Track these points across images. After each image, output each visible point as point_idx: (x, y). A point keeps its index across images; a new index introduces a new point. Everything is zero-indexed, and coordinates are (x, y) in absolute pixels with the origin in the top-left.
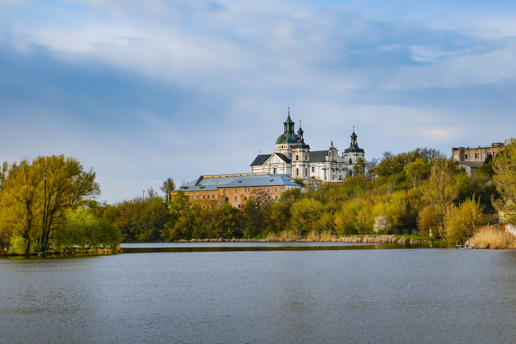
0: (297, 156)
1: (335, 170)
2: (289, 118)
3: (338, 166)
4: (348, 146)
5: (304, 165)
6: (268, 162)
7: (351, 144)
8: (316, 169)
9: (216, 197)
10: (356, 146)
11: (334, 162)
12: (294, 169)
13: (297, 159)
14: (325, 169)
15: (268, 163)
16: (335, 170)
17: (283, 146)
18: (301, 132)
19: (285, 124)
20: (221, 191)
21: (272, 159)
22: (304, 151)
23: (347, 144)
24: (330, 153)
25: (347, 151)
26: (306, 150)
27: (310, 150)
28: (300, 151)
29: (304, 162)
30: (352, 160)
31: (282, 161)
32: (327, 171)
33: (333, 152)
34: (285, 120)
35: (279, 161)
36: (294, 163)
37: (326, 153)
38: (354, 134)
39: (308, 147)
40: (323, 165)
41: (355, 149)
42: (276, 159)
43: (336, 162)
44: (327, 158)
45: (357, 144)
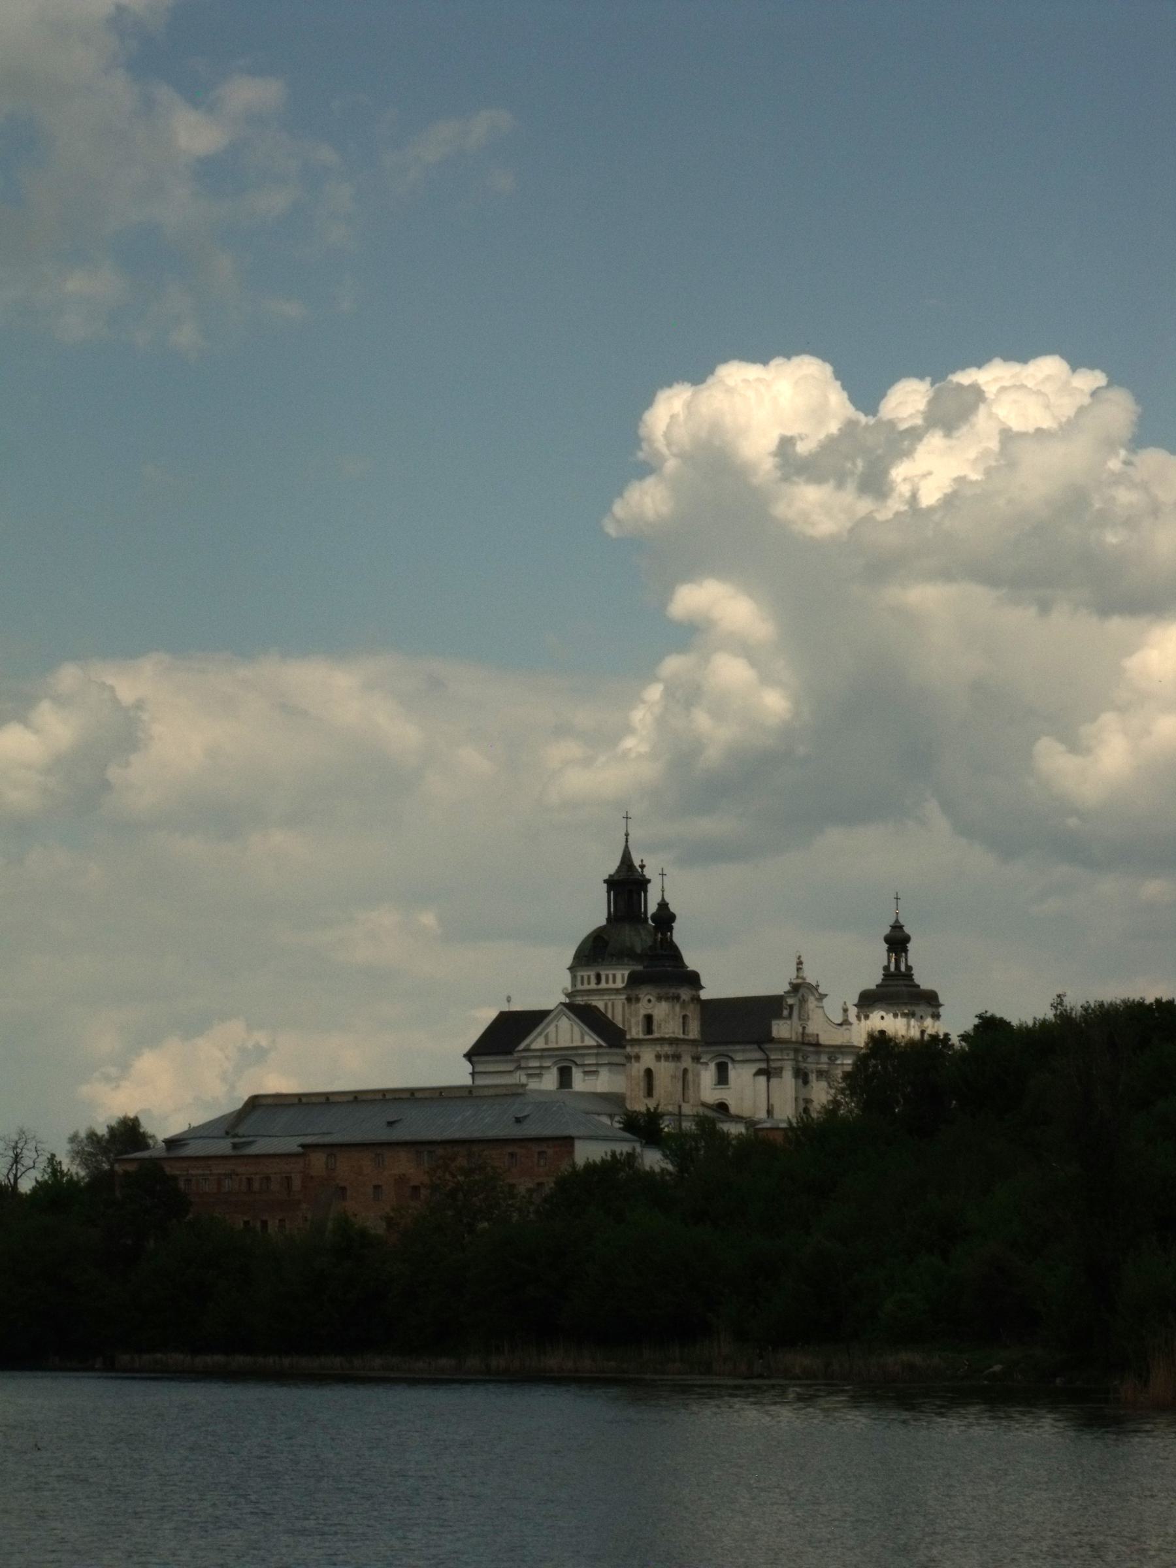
0: (649, 1019)
1: (813, 1077)
2: (626, 859)
3: (824, 1059)
4: (872, 979)
5: (677, 1057)
7: (886, 968)
8: (732, 1073)
10: (908, 975)
11: (808, 1045)
12: (637, 1069)
13: (649, 1029)
14: (766, 1073)
15: (539, 1044)
17: (598, 978)
19: (612, 883)
20: (318, 1161)
21: (552, 1028)
22: (677, 998)
23: (871, 967)
24: (791, 1007)
25: (868, 1001)
26: (685, 994)
27: (704, 995)
28: (659, 999)
29: (673, 1041)
31: (591, 1040)
32: (774, 1081)
33: (803, 1001)
34: (611, 866)
35: (583, 1040)
36: (636, 1049)
37: (770, 1007)
38: (897, 927)
39: (693, 980)
40: (758, 1055)
41: (898, 989)
42: (567, 1033)
43: (818, 1045)
44: (781, 1029)
45: (909, 968)
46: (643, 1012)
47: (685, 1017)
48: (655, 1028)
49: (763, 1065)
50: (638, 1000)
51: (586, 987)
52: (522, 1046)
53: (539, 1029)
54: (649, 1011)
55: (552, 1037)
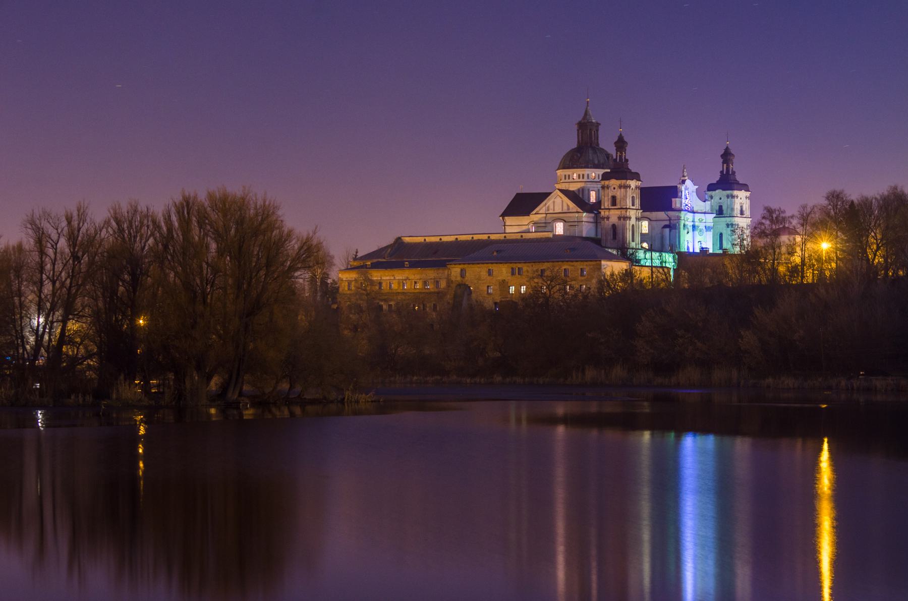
0: (614, 198)
2: (586, 113)
4: (715, 178)
6: (542, 208)
7: (722, 172)
9: (443, 284)
16: (691, 229)
18: (621, 144)
30: (724, 208)
34: (579, 118)
36: (607, 213)
46: (610, 195)
47: (633, 197)
48: (618, 201)
49: (667, 223)
50: (608, 187)
51: (567, 180)
52: (534, 212)
53: (544, 203)
54: (614, 194)
55: (551, 207)
